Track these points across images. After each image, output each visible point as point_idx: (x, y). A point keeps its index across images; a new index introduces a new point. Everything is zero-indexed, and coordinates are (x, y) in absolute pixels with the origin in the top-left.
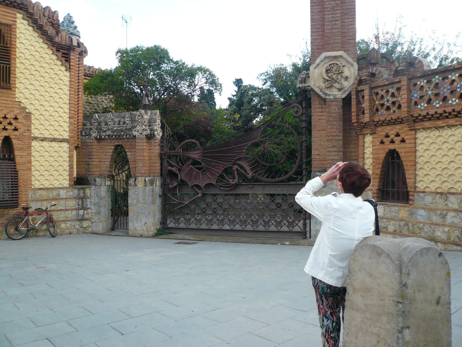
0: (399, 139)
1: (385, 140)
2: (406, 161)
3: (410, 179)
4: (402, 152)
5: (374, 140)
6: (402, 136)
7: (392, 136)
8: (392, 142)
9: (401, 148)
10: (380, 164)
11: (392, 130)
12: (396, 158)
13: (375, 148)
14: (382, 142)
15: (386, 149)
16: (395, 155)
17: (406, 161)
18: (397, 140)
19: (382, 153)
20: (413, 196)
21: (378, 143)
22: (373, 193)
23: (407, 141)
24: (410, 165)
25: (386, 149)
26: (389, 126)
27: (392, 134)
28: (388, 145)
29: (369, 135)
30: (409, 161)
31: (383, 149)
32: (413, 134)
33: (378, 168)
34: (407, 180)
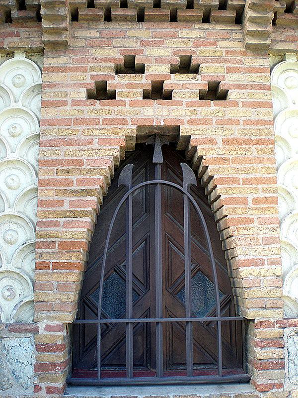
0: (193, 84)
1: (116, 82)
2: (234, 181)
3: (259, 263)
4: (213, 141)
5: (56, 77)
6: (209, 72)
7: (157, 70)
8: (158, 92)
9: (206, 122)
10: (88, 192)
11: (157, 45)
12: (158, 169)
13: (53, 113)
14: (102, 93)
15: (124, 122)
16: (158, 157)
17: (234, 181)
18: (185, 87)
19: (102, 142)
20: (278, 343)
21: (83, 95)
22: (40, 348)
23: (232, 95)
24: (256, 201)
25: (124, 122)
26: (141, 25)
27: (159, 60)
28: (133, 104)
29: (20, 57)
30: (247, 181)
31: (107, 121)
32: (260, 70)
33: (75, 214)
34: (244, 271)
